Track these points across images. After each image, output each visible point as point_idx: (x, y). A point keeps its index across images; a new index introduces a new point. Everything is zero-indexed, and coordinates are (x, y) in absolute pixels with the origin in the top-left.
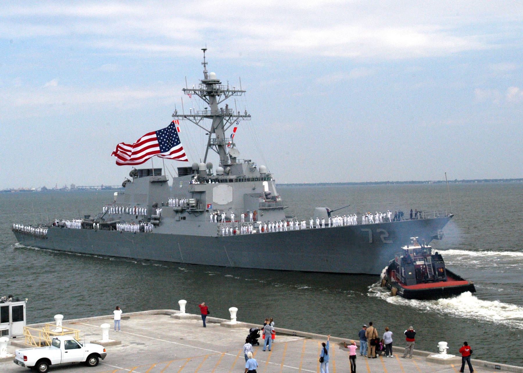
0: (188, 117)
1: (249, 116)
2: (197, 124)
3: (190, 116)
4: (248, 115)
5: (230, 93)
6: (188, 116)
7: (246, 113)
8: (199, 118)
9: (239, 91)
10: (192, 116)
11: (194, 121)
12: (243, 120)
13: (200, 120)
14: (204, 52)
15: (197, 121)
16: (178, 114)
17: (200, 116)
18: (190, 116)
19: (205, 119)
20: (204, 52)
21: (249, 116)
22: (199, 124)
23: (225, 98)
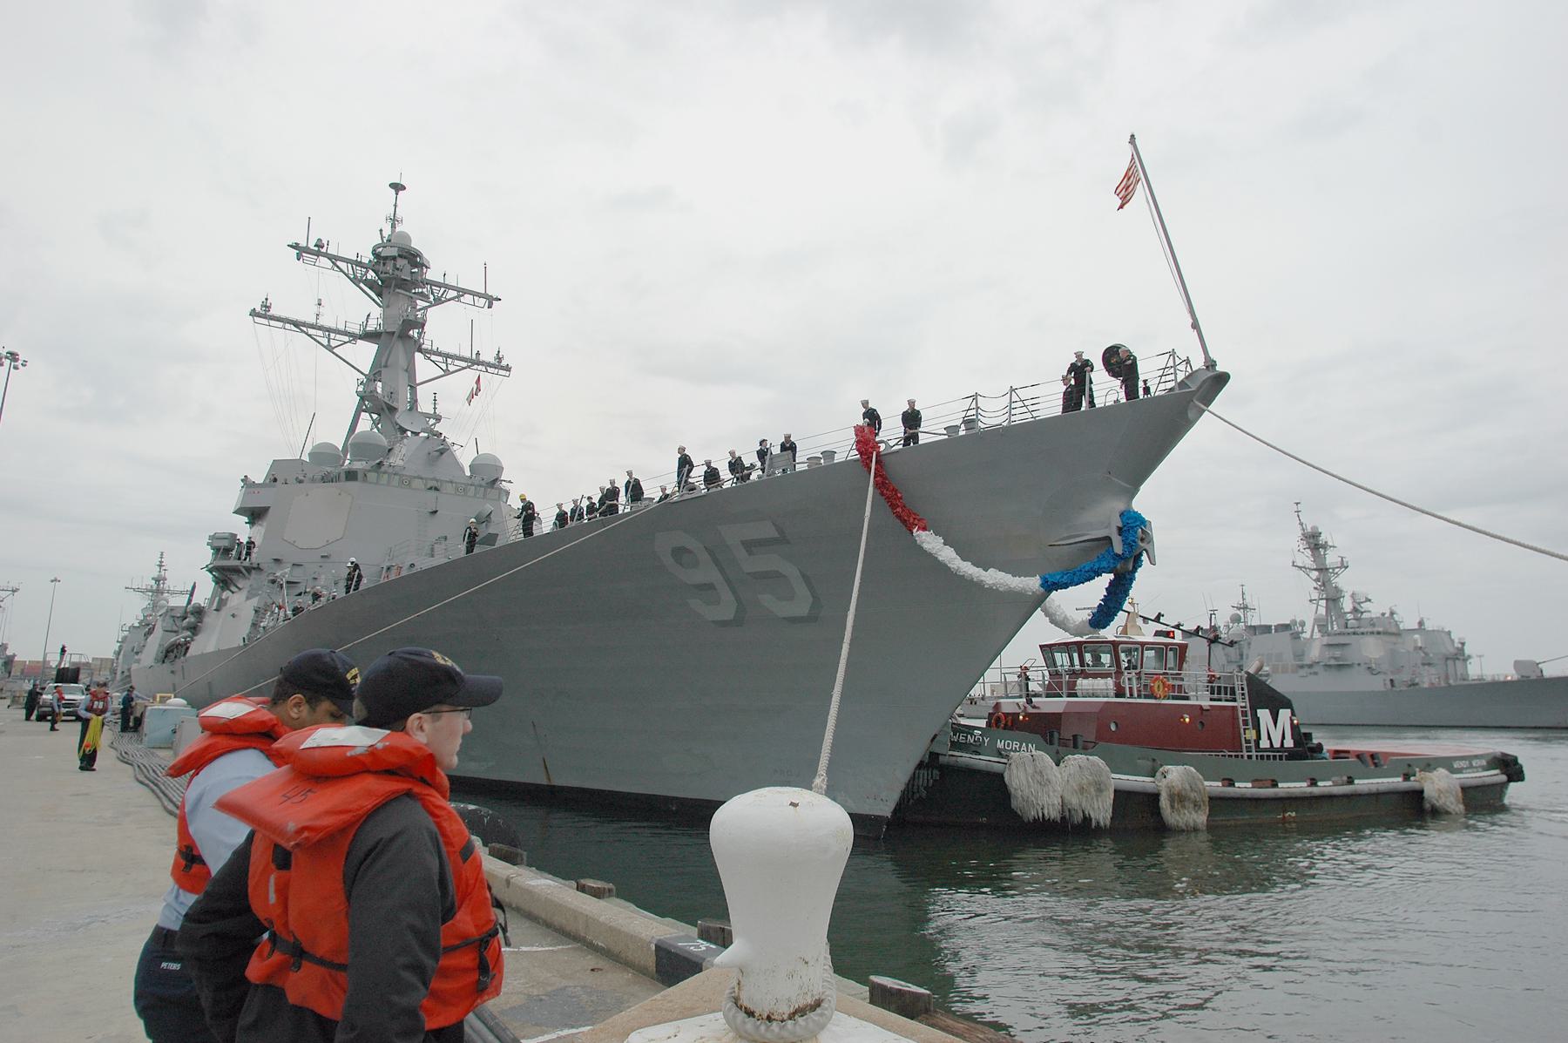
0: (305, 329)
1: (508, 369)
2: (330, 348)
3: (312, 326)
4: (504, 363)
5: (452, 294)
6: (304, 324)
7: (499, 359)
10: (320, 328)
11: (325, 341)
13: (346, 343)
14: (397, 194)
15: (333, 343)
16: (272, 312)
17: (345, 333)
18: (312, 326)
20: (397, 194)
21: (508, 369)
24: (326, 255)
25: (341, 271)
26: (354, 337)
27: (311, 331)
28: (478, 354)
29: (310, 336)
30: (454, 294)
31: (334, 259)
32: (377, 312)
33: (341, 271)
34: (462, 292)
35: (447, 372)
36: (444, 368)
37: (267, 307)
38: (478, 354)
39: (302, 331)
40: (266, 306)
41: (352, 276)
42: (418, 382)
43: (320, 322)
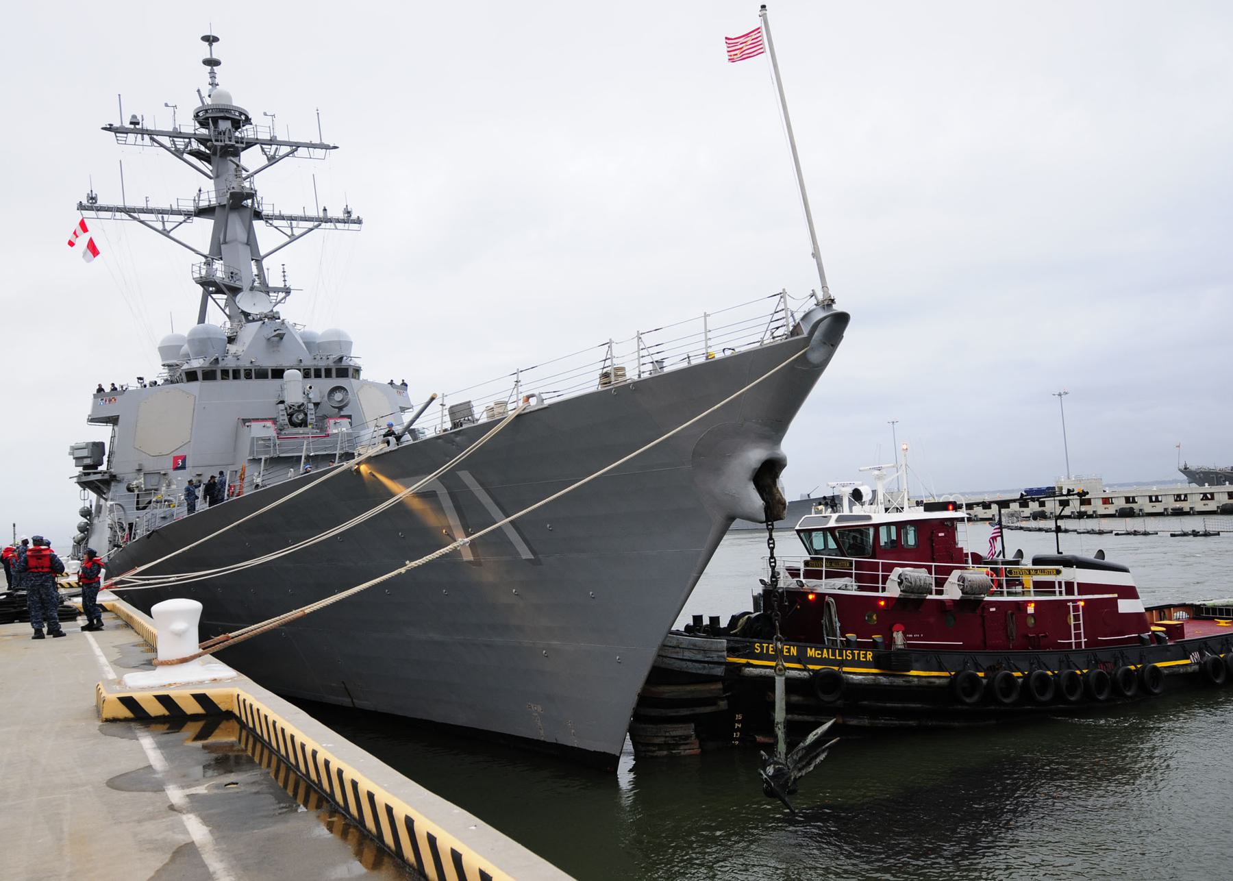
1: (359, 221)
2: (165, 233)
4: (354, 217)
5: (284, 150)
8: (181, 218)
9: (314, 146)
11: (159, 227)
12: (336, 229)
13: (181, 223)
14: (211, 45)
15: (169, 226)
16: (100, 202)
19: (196, 219)
21: (359, 221)
22: (171, 234)
23: (266, 162)
24: (143, 132)
25: (162, 145)
26: (189, 215)
27: (143, 217)
28: (325, 210)
29: (142, 222)
30: (288, 149)
31: (151, 134)
32: (209, 185)
33: (162, 145)
34: (296, 146)
35: (293, 238)
36: (289, 233)
37: (93, 199)
38: (325, 210)
39: (134, 218)
40: (92, 198)
41: (173, 149)
42: (262, 253)
43: (151, 205)
